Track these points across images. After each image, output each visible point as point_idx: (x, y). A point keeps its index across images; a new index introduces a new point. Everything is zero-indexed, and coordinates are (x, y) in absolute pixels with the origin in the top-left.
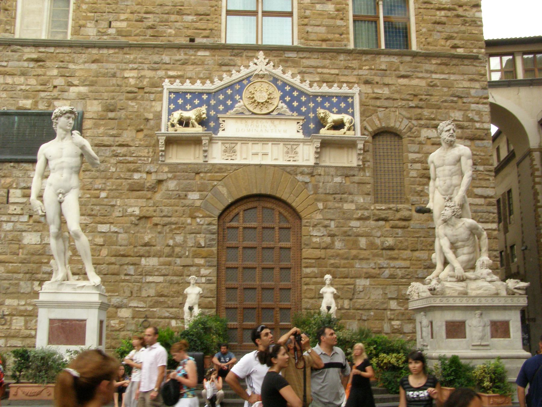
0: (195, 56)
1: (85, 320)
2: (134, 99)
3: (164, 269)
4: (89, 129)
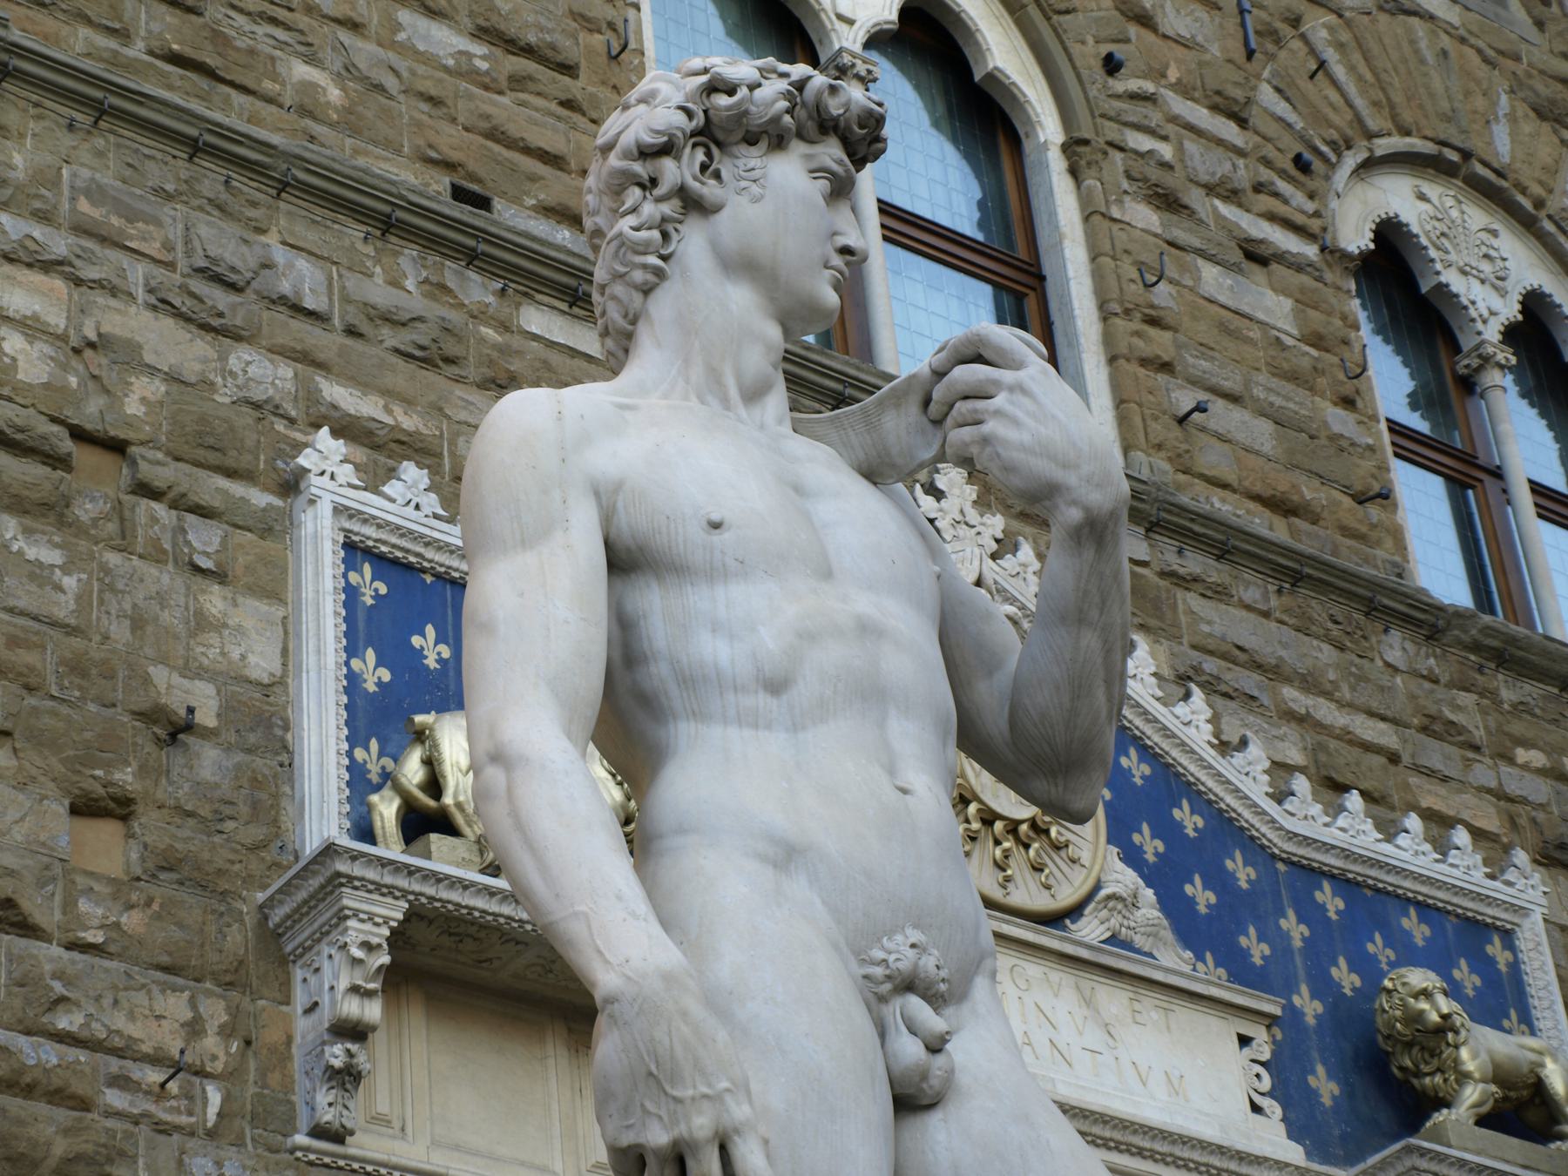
0: (504, 327)
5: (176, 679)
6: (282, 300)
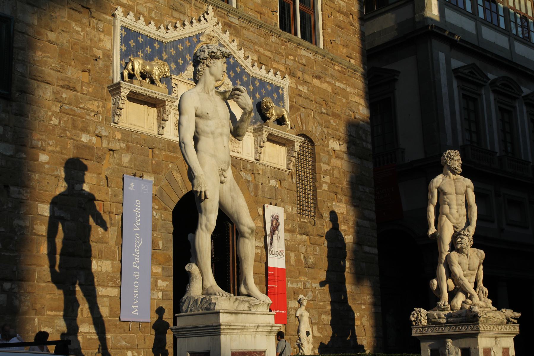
1: (265, 352)
5: (97, 50)
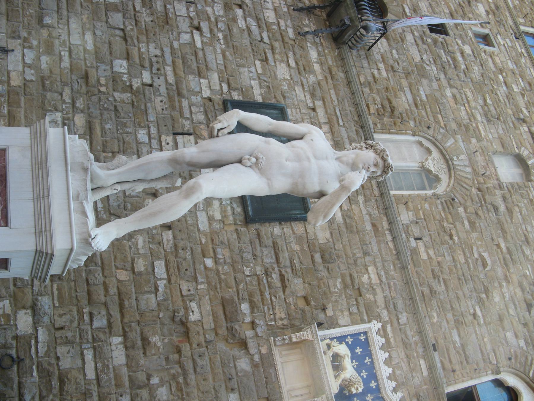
0: (418, 357)
2: (345, 286)
3: (108, 377)
4: (293, 231)
5: (331, 308)
6: (398, 317)
